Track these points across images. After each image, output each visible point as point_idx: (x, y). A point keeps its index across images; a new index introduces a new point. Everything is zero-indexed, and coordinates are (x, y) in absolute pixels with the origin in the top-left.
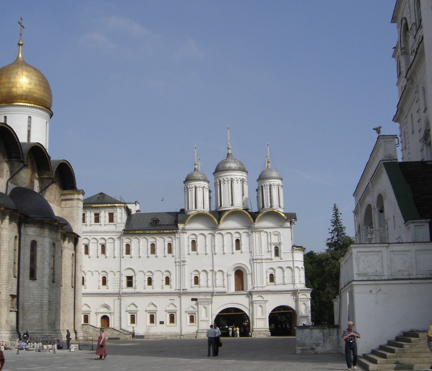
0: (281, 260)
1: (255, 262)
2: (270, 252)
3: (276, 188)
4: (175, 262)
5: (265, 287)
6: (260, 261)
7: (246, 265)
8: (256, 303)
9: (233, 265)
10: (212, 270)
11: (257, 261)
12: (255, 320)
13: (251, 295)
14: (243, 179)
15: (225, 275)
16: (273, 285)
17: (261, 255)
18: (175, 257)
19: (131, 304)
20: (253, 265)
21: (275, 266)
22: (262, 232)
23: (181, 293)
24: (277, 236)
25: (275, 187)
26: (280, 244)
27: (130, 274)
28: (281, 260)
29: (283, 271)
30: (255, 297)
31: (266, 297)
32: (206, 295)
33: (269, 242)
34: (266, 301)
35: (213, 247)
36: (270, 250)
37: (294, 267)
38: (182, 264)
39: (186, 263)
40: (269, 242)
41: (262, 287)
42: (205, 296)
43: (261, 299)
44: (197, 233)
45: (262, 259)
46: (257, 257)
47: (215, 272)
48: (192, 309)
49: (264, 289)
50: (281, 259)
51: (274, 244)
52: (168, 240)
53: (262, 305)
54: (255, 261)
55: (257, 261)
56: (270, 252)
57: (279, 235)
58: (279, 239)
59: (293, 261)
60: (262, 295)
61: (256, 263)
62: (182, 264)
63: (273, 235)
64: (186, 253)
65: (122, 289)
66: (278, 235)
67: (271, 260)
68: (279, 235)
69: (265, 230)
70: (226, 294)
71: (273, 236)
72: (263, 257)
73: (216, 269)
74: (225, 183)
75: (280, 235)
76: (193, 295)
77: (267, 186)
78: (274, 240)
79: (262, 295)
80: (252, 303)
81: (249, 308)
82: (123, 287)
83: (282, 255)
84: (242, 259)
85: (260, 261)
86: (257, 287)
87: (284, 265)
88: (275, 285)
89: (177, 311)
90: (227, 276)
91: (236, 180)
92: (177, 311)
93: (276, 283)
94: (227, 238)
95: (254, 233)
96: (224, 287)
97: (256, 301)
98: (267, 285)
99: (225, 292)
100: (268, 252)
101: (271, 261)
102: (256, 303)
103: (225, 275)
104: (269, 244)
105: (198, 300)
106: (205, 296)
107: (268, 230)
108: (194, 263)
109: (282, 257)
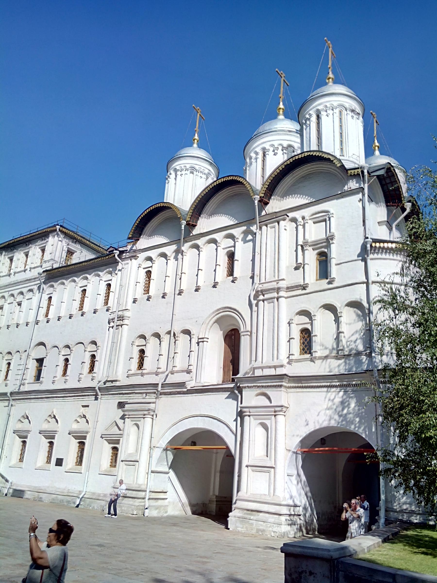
0: (331, 286)
1: (260, 300)
2: (301, 269)
3: (331, 116)
4: (109, 323)
5: (282, 366)
6: (275, 295)
7: (240, 311)
8: (249, 416)
9: (210, 315)
10: (169, 333)
11: (266, 296)
12: (244, 470)
13: (240, 390)
14: (290, 146)
15: (194, 341)
16: (306, 359)
17: (277, 279)
18: (110, 311)
19: (23, 416)
20: (255, 308)
21: (312, 303)
22: (284, 220)
23: (97, 388)
24: (324, 223)
25: (330, 112)
26: (328, 241)
27: (39, 353)
28: (331, 286)
29: (337, 320)
30: (250, 398)
31: (280, 397)
32: (146, 393)
33: (300, 242)
34: (278, 410)
35: (179, 276)
36: (300, 261)
37: (368, 302)
38: (119, 323)
39: (126, 322)
40: (300, 242)
41: (275, 367)
42: (144, 395)
43: (264, 401)
44: (153, 254)
45: (278, 290)
46: (266, 286)
47: (174, 334)
48: (115, 430)
49: (279, 371)
50: (330, 283)
51: (315, 245)
52: (105, 276)
53: (268, 422)
54: (261, 297)
55: (266, 296)
56: (301, 269)
57: (327, 219)
58: (328, 228)
59: (367, 283)
60: (269, 392)
61: (263, 301)
62: (119, 323)
63: (311, 222)
64: (131, 300)
65: (24, 385)
66: (324, 218)
67: (304, 289)
68: (327, 219)
69: (291, 215)
70: (185, 390)
71: (310, 225)
72: (282, 284)
73: (177, 329)
74: (251, 164)
75: (329, 220)
76: (120, 394)
77: (309, 119)
78: (315, 232)
79: (269, 392)
80: (241, 414)
81: (234, 430)
82: (26, 382)
83: (334, 271)
84: (236, 297)
85: (275, 295)
86: (262, 368)
87: (338, 298)
88: (312, 360)
89: (87, 432)
90: (198, 343)
91: (272, 149)
92: (87, 432)
93: (314, 355)
94: (207, 250)
95: (264, 228)
96: (189, 372)
97: (251, 410)
98: (289, 363)
99: (182, 385)
100: (296, 268)
101: (304, 292)
102: (249, 416)
103: (194, 341)
104: (299, 247)
105: (126, 405)
106: (144, 395)
107: (297, 215)
108: (144, 318)
109: (332, 277)
